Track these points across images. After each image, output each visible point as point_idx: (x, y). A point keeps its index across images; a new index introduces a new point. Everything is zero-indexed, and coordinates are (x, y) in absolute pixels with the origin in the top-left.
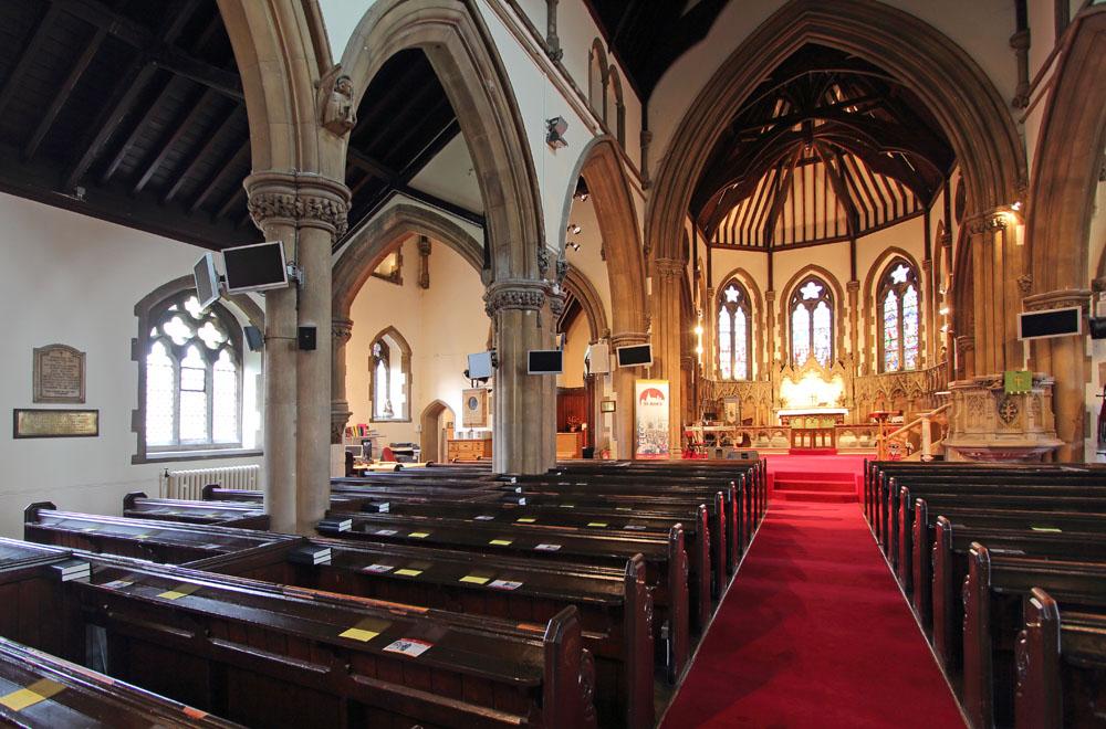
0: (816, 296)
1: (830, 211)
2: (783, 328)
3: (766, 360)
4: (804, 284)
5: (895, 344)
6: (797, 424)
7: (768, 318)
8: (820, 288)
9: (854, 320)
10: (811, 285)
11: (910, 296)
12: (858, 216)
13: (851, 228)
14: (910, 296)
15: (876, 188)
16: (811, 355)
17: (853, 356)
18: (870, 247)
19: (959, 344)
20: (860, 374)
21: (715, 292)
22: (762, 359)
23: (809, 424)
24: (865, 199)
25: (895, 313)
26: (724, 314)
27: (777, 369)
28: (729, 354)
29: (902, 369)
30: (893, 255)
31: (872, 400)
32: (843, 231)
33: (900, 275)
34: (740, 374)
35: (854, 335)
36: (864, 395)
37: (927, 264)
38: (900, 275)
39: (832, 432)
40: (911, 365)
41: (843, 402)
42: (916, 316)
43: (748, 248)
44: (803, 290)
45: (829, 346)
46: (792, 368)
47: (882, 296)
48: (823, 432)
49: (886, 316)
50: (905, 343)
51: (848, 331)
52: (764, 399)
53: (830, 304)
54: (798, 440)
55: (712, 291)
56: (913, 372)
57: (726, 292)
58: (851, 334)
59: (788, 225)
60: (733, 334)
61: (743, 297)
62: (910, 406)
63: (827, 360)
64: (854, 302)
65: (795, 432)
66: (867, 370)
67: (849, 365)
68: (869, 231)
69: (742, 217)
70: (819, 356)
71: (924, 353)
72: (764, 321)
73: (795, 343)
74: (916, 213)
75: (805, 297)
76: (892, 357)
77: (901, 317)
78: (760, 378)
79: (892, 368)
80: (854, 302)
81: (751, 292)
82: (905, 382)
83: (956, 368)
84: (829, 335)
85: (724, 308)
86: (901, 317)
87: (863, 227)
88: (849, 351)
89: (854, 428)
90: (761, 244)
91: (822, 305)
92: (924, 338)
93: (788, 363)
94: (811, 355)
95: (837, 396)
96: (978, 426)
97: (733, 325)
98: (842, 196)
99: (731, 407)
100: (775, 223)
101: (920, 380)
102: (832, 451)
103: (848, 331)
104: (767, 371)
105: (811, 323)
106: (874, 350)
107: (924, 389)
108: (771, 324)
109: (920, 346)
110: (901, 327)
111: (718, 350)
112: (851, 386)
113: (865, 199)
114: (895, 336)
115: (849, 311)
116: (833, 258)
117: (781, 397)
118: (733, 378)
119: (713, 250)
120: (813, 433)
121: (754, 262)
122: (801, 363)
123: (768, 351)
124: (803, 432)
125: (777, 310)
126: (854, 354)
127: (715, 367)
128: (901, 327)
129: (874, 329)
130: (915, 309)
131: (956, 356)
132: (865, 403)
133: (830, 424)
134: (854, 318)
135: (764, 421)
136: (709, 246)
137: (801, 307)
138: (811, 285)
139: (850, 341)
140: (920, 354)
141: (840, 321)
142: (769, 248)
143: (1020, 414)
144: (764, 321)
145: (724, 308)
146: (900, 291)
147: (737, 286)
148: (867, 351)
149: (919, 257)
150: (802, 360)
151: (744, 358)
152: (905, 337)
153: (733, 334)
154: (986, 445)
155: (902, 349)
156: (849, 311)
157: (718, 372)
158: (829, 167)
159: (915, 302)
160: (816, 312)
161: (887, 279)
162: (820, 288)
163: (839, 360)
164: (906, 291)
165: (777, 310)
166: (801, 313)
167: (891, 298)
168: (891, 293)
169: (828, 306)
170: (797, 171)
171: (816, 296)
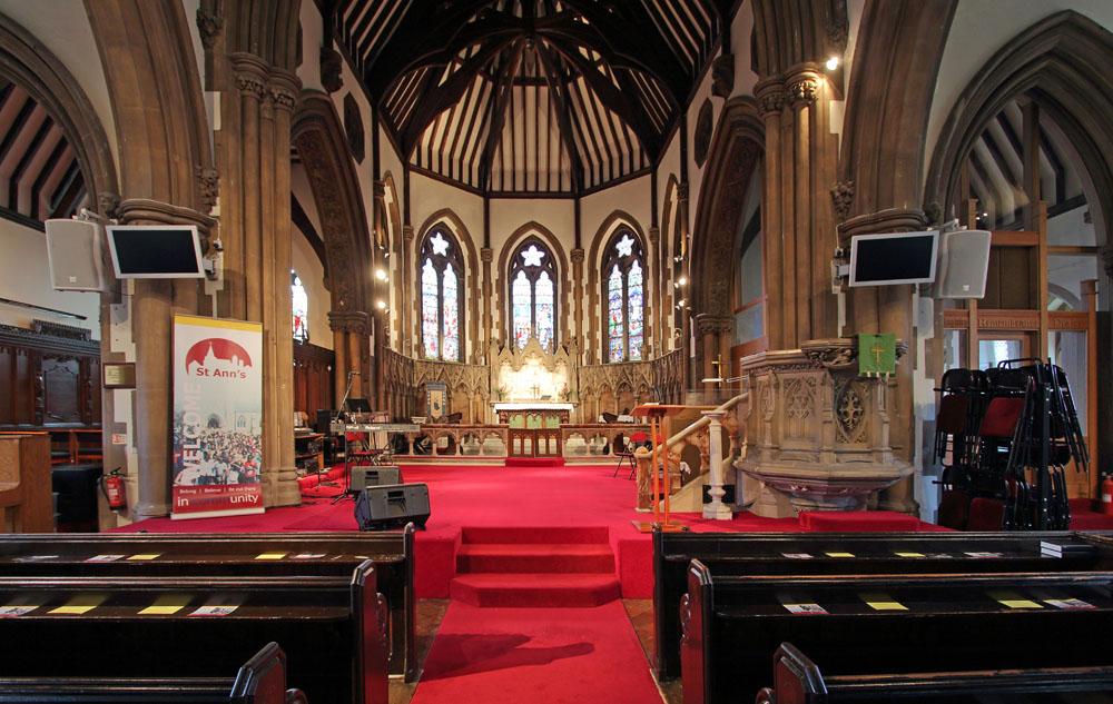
0: (538, 263)
1: (556, 161)
2: (502, 298)
3: (481, 338)
4: (525, 246)
5: (620, 329)
6: (517, 423)
7: (484, 283)
8: (542, 254)
9: (578, 297)
10: (533, 249)
11: (636, 272)
12: (582, 170)
13: (575, 183)
14: (636, 272)
15: (605, 130)
16: (534, 335)
17: (578, 340)
18: (597, 206)
19: (698, 324)
20: (584, 364)
21: (416, 234)
22: (476, 335)
23: (534, 423)
24: (601, 145)
25: (620, 293)
26: (429, 270)
27: (494, 350)
28: (436, 325)
29: (627, 359)
30: (619, 221)
31: (596, 395)
32: (567, 187)
33: (625, 246)
34: (450, 353)
35: (579, 316)
36: (589, 388)
37: (654, 234)
38: (625, 246)
39: (558, 434)
40: (636, 355)
41: (566, 396)
42: (640, 297)
43: (459, 184)
44: (524, 254)
45: (551, 326)
46: (511, 349)
47: (607, 272)
48: (547, 433)
49: (611, 295)
50: (630, 329)
51: (572, 309)
52: (479, 388)
53: (553, 277)
54: (517, 442)
55: (411, 231)
56: (639, 363)
57: (432, 239)
58: (575, 313)
59: (508, 166)
60: (440, 298)
61: (454, 249)
63: (550, 343)
64: (578, 276)
65: (513, 433)
66: (592, 359)
67: (573, 350)
68: (594, 189)
69: (444, 134)
70: (542, 338)
71: (651, 341)
72: (480, 286)
73: (515, 320)
74: (642, 172)
75: (527, 263)
76: (617, 344)
77: (626, 298)
78: (475, 361)
79: (616, 358)
80: (578, 276)
81: (463, 245)
83: (693, 355)
84: (552, 313)
85: (429, 261)
86: (626, 298)
87: (588, 185)
88: (573, 334)
89: (577, 429)
90: (475, 184)
91: (544, 275)
92: (651, 323)
93: (507, 342)
94: (534, 335)
95: (560, 388)
96: (801, 437)
97: (440, 287)
98: (566, 135)
99: (436, 396)
100: (492, 157)
101: (646, 370)
102: (556, 462)
103: (572, 309)
104: (482, 349)
105: (533, 296)
106: (599, 335)
107: (650, 384)
108: (488, 295)
109: (646, 333)
110: (626, 309)
111: (421, 318)
112: (575, 376)
113: (601, 145)
114: (620, 320)
115: (573, 285)
116: (555, 216)
117: (500, 386)
118: (440, 357)
119: (412, 174)
120: (535, 435)
121: (467, 206)
122: (521, 346)
123: (484, 326)
124: (523, 433)
125: (495, 275)
126: (579, 338)
127: (415, 340)
128: (626, 309)
129: (598, 308)
130: (640, 289)
131: (693, 340)
132: (589, 399)
133: (554, 423)
134: (578, 297)
135: (480, 419)
136: (407, 168)
137: (522, 275)
138: (533, 249)
139: (574, 323)
140: (645, 342)
141: (564, 297)
142: (486, 194)
143: (866, 418)
144: (480, 286)
145: (429, 261)
146: (625, 267)
147: (447, 236)
148: (591, 335)
149: (646, 225)
150: (523, 342)
151: (455, 332)
153: (440, 298)
154: (824, 474)
155: (627, 336)
156: (573, 285)
157: (420, 347)
158: (552, 94)
159: (640, 280)
160: (537, 282)
161: (611, 250)
162: (542, 254)
163: (563, 344)
164: (630, 266)
165: (495, 275)
166: (521, 283)
167: (616, 274)
168: (616, 268)
169: (551, 277)
170: (517, 90)
171: (538, 263)
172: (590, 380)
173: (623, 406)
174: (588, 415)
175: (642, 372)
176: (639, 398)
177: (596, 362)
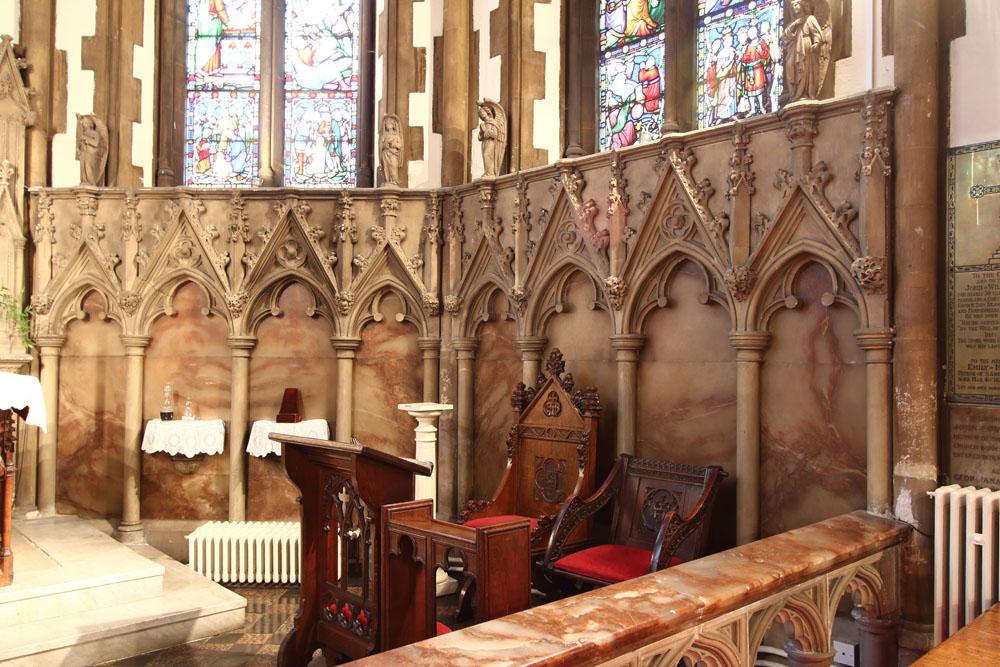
5: (243, 58)
31: (133, 326)
36: (87, 292)
62: (346, 367)
66: (106, 167)
82: (334, 245)
101: (407, 228)
106: (143, 63)
126: (38, 59)
132: (90, 340)
148: (107, 54)
152: (292, 28)
172: (99, 250)
173: (275, 383)
174: (81, 415)
175: (390, 235)
176: (358, 347)
177: (124, 177)
